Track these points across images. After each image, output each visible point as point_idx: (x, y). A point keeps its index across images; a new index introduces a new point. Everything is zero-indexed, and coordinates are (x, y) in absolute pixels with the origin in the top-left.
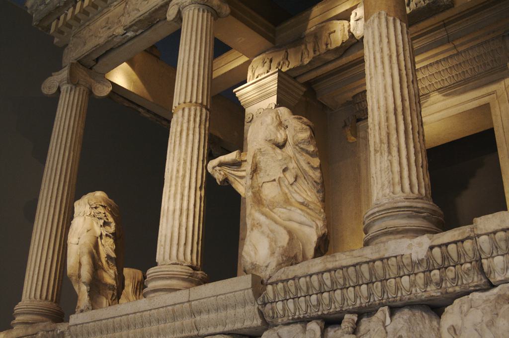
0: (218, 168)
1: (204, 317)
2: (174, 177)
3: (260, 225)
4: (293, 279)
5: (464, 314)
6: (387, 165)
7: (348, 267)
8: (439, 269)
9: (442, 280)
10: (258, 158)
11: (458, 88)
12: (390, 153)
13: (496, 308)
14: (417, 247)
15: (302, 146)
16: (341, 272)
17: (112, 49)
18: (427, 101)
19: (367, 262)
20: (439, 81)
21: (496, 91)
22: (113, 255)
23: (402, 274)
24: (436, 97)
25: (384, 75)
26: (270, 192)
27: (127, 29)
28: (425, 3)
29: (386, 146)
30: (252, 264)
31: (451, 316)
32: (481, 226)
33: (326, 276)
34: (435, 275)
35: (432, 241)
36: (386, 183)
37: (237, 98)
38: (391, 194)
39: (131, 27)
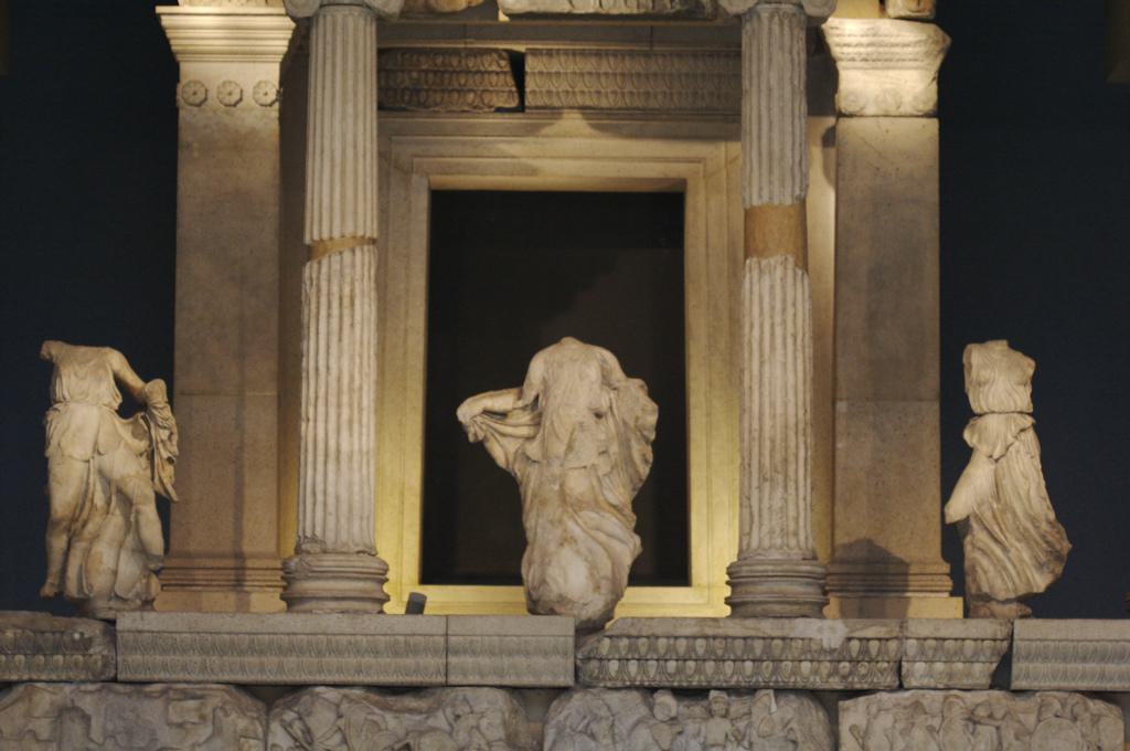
0: (479, 419)
1: (469, 660)
3: (576, 541)
4: (648, 637)
5: (871, 718)
6: (780, 505)
7: (734, 638)
8: (850, 662)
9: (851, 673)
10: (576, 433)
11: (628, 122)
12: (786, 487)
13: (912, 716)
14: (829, 630)
15: (646, 433)
16: (724, 642)
18: (551, 124)
19: (764, 638)
20: (590, 92)
21: (705, 159)
23: (803, 657)
24: (573, 122)
26: (578, 484)
28: (672, 7)
29: (780, 477)
30: (561, 596)
31: (853, 714)
32: (913, 629)
33: (700, 642)
34: (844, 667)
35: (852, 631)
36: (778, 530)
38: (785, 548)
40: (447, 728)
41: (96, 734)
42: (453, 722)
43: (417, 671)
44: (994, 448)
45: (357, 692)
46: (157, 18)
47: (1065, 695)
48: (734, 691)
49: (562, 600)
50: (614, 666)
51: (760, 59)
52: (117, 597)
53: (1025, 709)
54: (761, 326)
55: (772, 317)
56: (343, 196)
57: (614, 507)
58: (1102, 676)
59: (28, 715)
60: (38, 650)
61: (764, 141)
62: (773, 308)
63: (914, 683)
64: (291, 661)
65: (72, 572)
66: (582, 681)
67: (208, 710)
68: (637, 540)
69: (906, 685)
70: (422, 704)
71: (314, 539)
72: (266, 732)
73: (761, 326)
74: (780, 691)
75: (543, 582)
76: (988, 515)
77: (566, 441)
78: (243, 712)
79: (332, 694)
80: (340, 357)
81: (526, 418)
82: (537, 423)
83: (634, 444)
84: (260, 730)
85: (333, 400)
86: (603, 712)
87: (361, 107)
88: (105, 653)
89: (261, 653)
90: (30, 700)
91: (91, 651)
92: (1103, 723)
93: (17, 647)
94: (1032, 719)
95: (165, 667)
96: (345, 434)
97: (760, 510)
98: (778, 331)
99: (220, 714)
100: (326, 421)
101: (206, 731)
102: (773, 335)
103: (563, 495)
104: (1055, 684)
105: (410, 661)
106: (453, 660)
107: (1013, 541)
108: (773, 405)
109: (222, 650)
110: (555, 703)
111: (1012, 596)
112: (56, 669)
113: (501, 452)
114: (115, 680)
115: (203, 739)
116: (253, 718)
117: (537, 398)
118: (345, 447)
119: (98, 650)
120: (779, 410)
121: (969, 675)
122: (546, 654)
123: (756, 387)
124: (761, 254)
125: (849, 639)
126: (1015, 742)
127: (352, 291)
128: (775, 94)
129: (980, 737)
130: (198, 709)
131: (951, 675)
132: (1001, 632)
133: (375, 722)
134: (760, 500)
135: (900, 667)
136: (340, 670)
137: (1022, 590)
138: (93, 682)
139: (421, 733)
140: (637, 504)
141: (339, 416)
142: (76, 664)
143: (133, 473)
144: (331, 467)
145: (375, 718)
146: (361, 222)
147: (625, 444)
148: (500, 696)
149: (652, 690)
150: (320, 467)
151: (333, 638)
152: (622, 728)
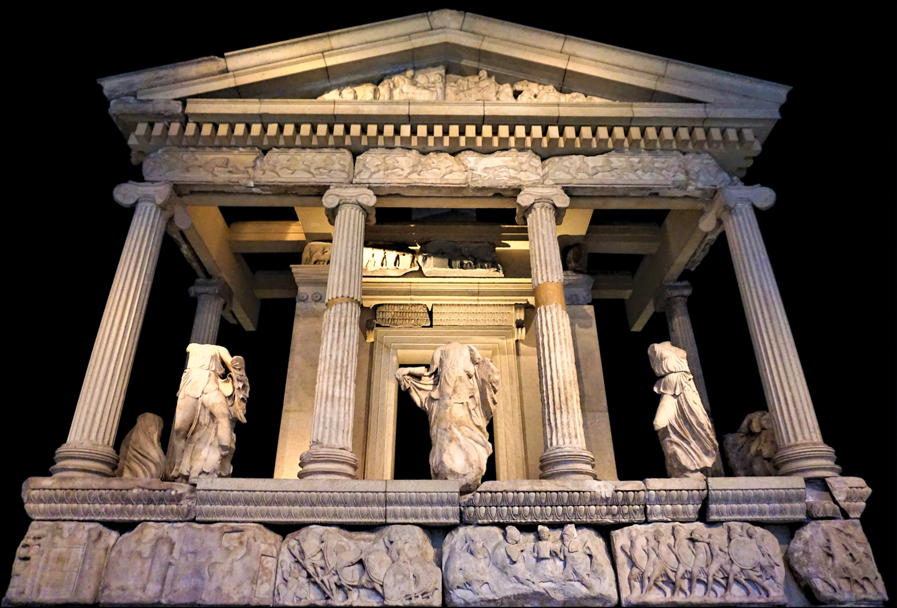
0: (407, 377)
1: (399, 508)
2: (339, 365)
7: (551, 492)
9: (618, 513)
17: (223, 192)
22: (244, 421)
25: (561, 353)
26: (459, 412)
31: (620, 538)
37: (292, 274)
39: (264, 185)
40: (384, 549)
41: (176, 554)
42: (389, 546)
43: (368, 515)
44: (675, 389)
45: (334, 528)
46: (290, 269)
47: (741, 524)
48: (553, 526)
49: (453, 473)
50: (483, 509)
51: (537, 225)
52: (203, 472)
53: (718, 535)
55: (553, 330)
56: (344, 279)
57: (478, 427)
58: (761, 512)
59: (139, 542)
60: (150, 501)
62: (553, 326)
63: (654, 519)
64: (296, 509)
65: (186, 461)
66: (464, 523)
67: (245, 538)
70: (372, 536)
74: (579, 526)
75: (442, 462)
78: (265, 542)
79: (321, 529)
80: (338, 349)
81: (431, 381)
82: (435, 384)
85: (333, 371)
86: (477, 539)
88: (190, 503)
89: (279, 503)
91: (182, 502)
93: (138, 500)
94: (725, 537)
97: (556, 424)
99: (252, 540)
100: (328, 382)
101: (243, 551)
103: (451, 418)
105: (365, 508)
106: (389, 508)
107: (691, 439)
109: (257, 503)
111: (698, 468)
113: (419, 398)
114: (194, 521)
116: (270, 544)
118: (337, 394)
119: (185, 504)
120: (561, 374)
121: (684, 513)
122: (441, 503)
124: (545, 304)
125: (617, 491)
127: (346, 320)
128: (546, 238)
129: (699, 550)
130: (239, 538)
131: (675, 513)
132: (702, 486)
133: (343, 547)
135: (645, 509)
136: (324, 515)
138: (181, 522)
139: (369, 553)
141: (335, 378)
142: (172, 510)
143: (218, 401)
144: (329, 403)
145: (343, 543)
146: (352, 291)
148: (417, 528)
150: (323, 404)
151: (320, 494)
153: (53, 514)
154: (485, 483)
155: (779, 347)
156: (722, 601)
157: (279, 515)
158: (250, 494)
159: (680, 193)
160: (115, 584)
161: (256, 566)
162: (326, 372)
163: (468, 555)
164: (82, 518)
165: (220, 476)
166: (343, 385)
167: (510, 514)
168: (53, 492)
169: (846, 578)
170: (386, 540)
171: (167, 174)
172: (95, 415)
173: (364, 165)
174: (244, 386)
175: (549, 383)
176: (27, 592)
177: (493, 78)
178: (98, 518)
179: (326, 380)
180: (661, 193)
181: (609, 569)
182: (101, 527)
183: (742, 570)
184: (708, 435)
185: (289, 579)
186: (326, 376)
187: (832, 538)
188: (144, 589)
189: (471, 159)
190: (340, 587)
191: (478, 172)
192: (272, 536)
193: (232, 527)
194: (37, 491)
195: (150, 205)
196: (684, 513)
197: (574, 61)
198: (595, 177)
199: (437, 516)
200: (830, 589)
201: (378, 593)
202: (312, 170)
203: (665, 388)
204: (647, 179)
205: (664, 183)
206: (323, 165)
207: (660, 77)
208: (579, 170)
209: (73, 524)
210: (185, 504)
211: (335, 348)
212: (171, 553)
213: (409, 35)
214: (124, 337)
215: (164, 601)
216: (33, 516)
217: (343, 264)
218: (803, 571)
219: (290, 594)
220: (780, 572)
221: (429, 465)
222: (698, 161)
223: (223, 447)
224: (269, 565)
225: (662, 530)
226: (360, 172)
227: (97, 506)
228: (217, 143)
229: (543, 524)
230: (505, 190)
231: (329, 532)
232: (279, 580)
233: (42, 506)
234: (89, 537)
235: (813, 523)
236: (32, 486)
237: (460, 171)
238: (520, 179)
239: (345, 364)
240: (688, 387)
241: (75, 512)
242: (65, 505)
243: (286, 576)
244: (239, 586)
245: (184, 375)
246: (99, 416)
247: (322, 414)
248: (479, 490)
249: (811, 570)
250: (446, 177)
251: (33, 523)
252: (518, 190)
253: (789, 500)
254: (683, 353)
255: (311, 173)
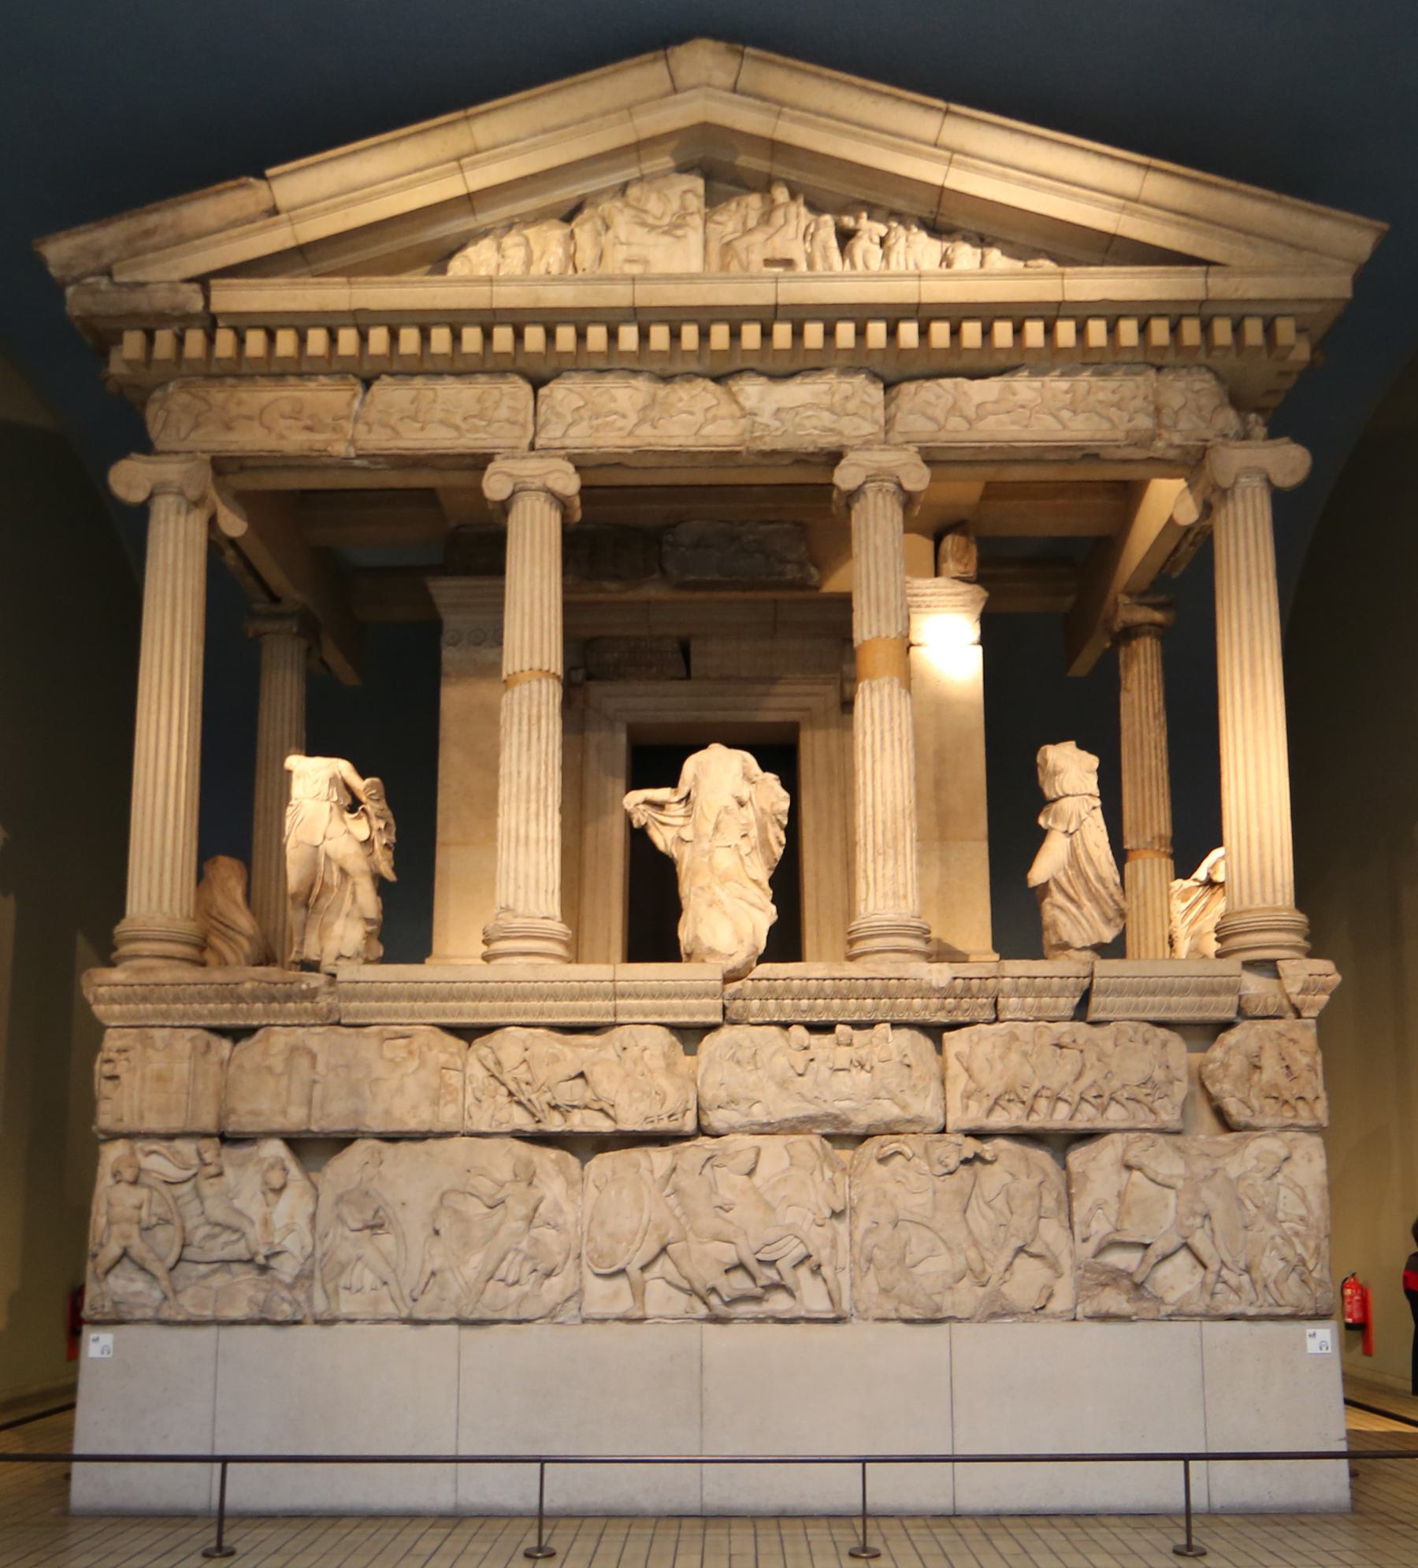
0: (642, 807)
22: (391, 876)
25: (893, 762)
26: (725, 860)
27: (359, 457)
29: (891, 852)
39: (374, 455)
41: (320, 1067)
44: (1069, 823)
48: (857, 1025)
49: (712, 952)
50: (756, 1003)
51: (867, 527)
52: (340, 957)
54: (873, 733)
55: (882, 724)
56: (531, 638)
57: (755, 881)
58: (1169, 1008)
59: (266, 1053)
60: (272, 999)
61: (873, 587)
62: (882, 717)
63: (1009, 1017)
64: (484, 1005)
68: (773, 908)
69: (1001, 1017)
71: (507, 909)
72: (464, 1066)
73: (873, 733)
74: (895, 1025)
75: (696, 938)
76: (1064, 881)
77: (713, 821)
78: (444, 1050)
80: (529, 759)
83: (769, 826)
84: (459, 1063)
85: (523, 797)
86: (747, 1043)
87: (546, 570)
88: (330, 1000)
90: (268, 1040)
92: (1170, 1046)
93: (255, 997)
95: (380, 1013)
96: (533, 824)
98: (887, 735)
99: (425, 1049)
100: (518, 814)
102: (882, 738)
104: (1127, 1015)
106: (620, 1002)
107: (1085, 901)
108: (883, 794)
109: (428, 997)
110: (706, 1038)
112: (290, 1015)
113: (662, 839)
114: (338, 1024)
115: (410, 1071)
116: (452, 1054)
117: (689, 794)
118: (533, 835)
119: (323, 1002)
121: (1055, 1008)
123: (869, 782)
124: (871, 677)
126: (1097, 1064)
127: (539, 711)
128: (881, 551)
131: (1040, 1009)
134: (875, 871)
135: (996, 1004)
136: (525, 1013)
137: (1095, 941)
139: (594, 1064)
140: (772, 882)
141: (528, 809)
142: (306, 1010)
144: (522, 849)
147: (763, 829)
149: (786, 1026)
152: (763, 1056)
153: (133, 1018)
154: (762, 966)
155: (1256, 753)
156: (1089, 1125)
157: (461, 1014)
158: (416, 986)
159: (1140, 454)
160: (243, 1107)
161: (435, 1081)
162: (513, 799)
163: (733, 1065)
164: (177, 1024)
165: (367, 962)
166: (542, 819)
167: (796, 1009)
168: (129, 989)
169: (1276, 1098)
170: (617, 1045)
171: (193, 436)
172: (161, 875)
173: (553, 407)
174: (386, 825)
175: (870, 812)
176: (125, 1118)
177: (801, 200)
178: (201, 1023)
179: (514, 810)
180: (1103, 453)
181: (935, 1086)
182: (206, 1035)
183: (1124, 1086)
184: (1111, 896)
185: (483, 1098)
186: (514, 805)
187: (1267, 1045)
188: (284, 1113)
189: (752, 391)
190: (555, 1107)
191: (765, 418)
192: (454, 1043)
193: (396, 1032)
194: (106, 989)
195: (171, 499)
196: (1055, 1008)
197: (960, 165)
198: (981, 425)
199: (692, 1014)
200: (1248, 1112)
201: (607, 1115)
202: (457, 419)
203: (1055, 820)
204: (1080, 429)
205: (1110, 435)
206: (475, 409)
207: (1131, 202)
208: (954, 409)
209: (166, 1032)
210: (323, 1002)
211: (524, 758)
212: (313, 1065)
213: (629, 107)
214: (180, 747)
215: (314, 1128)
216: (106, 1022)
217: (527, 610)
218: (1214, 1089)
219: (487, 1117)
220: (1181, 1090)
221: (677, 941)
222: (1181, 385)
223: (368, 921)
224: (453, 1081)
225: (1018, 1032)
226: (547, 422)
227: (196, 1006)
228: (275, 369)
229: (842, 1023)
230: (812, 454)
231: (534, 1037)
232: (470, 1099)
233: (116, 1008)
234: (194, 1048)
235: (1246, 1023)
236: (97, 980)
237: (732, 417)
238: (840, 433)
239: (543, 785)
240: (1089, 819)
241: (165, 1015)
242: (149, 1006)
243: (479, 1095)
244: (414, 1107)
245: (289, 810)
246: (167, 876)
247: (512, 867)
248: (751, 976)
249: (1227, 1086)
250: (704, 432)
251: (109, 1031)
252: (834, 457)
253: (1214, 991)
254: (1093, 761)
255: (457, 428)
